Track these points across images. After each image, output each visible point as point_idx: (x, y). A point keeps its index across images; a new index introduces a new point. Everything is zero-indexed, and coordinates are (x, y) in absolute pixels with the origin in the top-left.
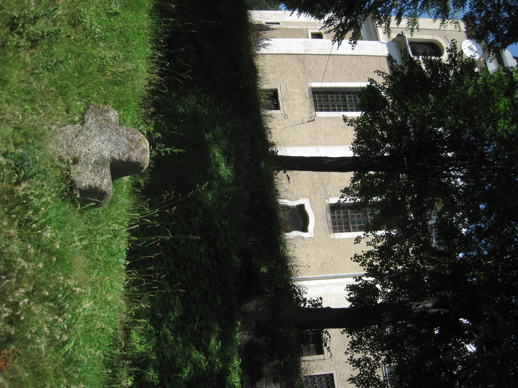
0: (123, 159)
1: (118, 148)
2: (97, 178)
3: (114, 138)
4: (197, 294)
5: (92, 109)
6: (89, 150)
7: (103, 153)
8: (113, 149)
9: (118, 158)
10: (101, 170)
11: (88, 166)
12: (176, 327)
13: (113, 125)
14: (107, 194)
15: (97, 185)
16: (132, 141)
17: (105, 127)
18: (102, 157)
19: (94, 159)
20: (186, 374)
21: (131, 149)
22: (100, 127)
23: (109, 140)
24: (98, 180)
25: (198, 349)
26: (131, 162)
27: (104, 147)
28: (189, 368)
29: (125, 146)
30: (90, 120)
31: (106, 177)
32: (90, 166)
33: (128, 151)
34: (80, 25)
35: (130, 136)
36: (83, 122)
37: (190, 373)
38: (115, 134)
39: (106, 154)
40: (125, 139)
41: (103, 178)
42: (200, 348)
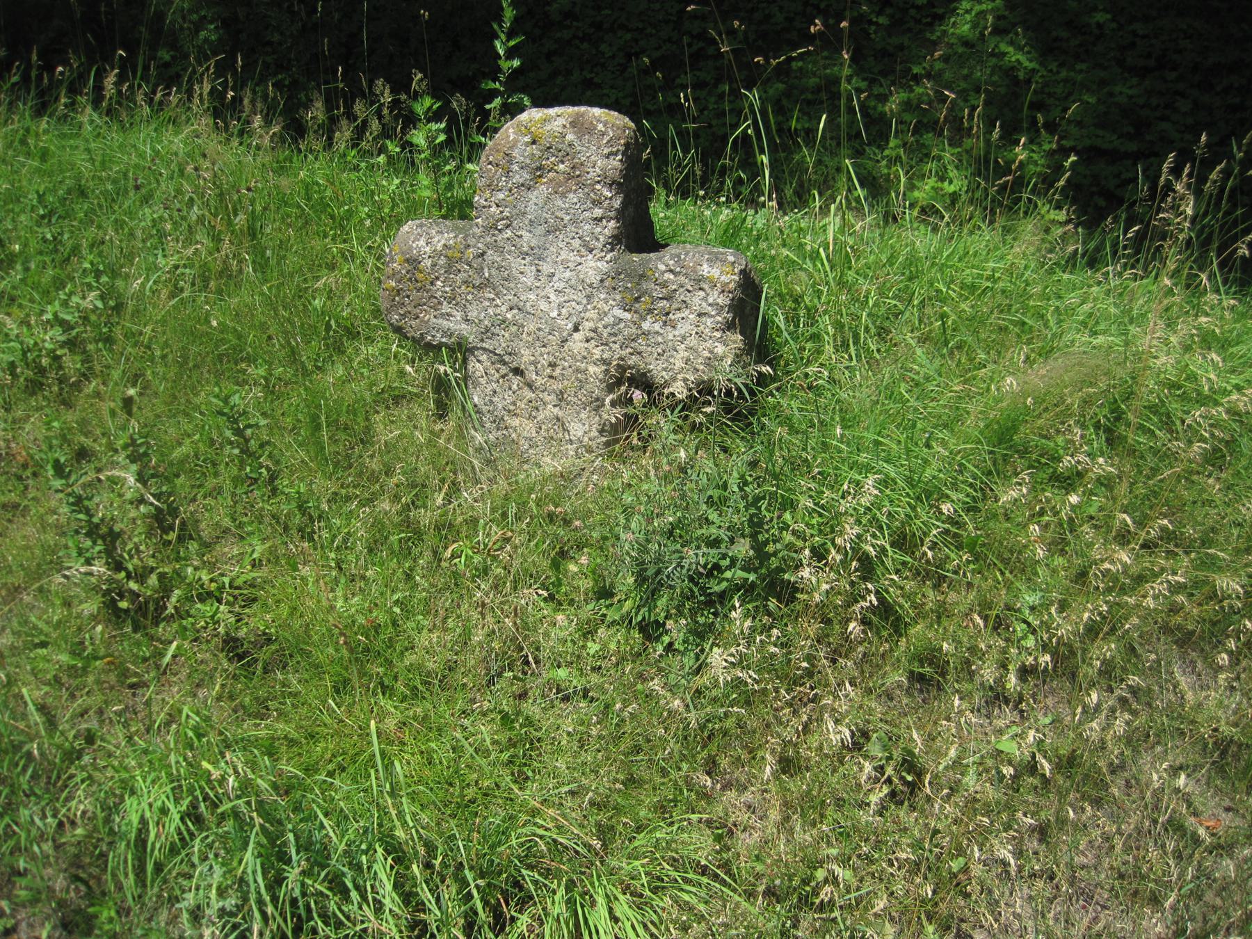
0: (617, 203)
1: (573, 222)
2: (696, 300)
3: (528, 239)
4: (781, 8)
5: (403, 316)
6: (576, 329)
7: (594, 278)
8: (576, 243)
9: (612, 224)
10: (664, 285)
11: (646, 334)
12: (884, 73)
13: (471, 241)
14: (1071, 263)
15: (723, 300)
16: (538, 172)
17: (480, 271)
18: (610, 281)
19: (618, 312)
20: (1020, 57)
21: (575, 176)
22: (480, 287)
23: (536, 255)
24: (705, 299)
25: (941, 18)
26: (625, 177)
27: (568, 274)
28: (1004, 47)
29: (563, 195)
30: (452, 323)
31: (695, 271)
32: (646, 326)
33: (581, 185)
34: (477, 367)
35: (517, 179)
36: (461, 351)
37: (1020, 48)
38: (509, 233)
39: (595, 266)
40: (533, 196)
41: (699, 281)
42: (940, 11)
